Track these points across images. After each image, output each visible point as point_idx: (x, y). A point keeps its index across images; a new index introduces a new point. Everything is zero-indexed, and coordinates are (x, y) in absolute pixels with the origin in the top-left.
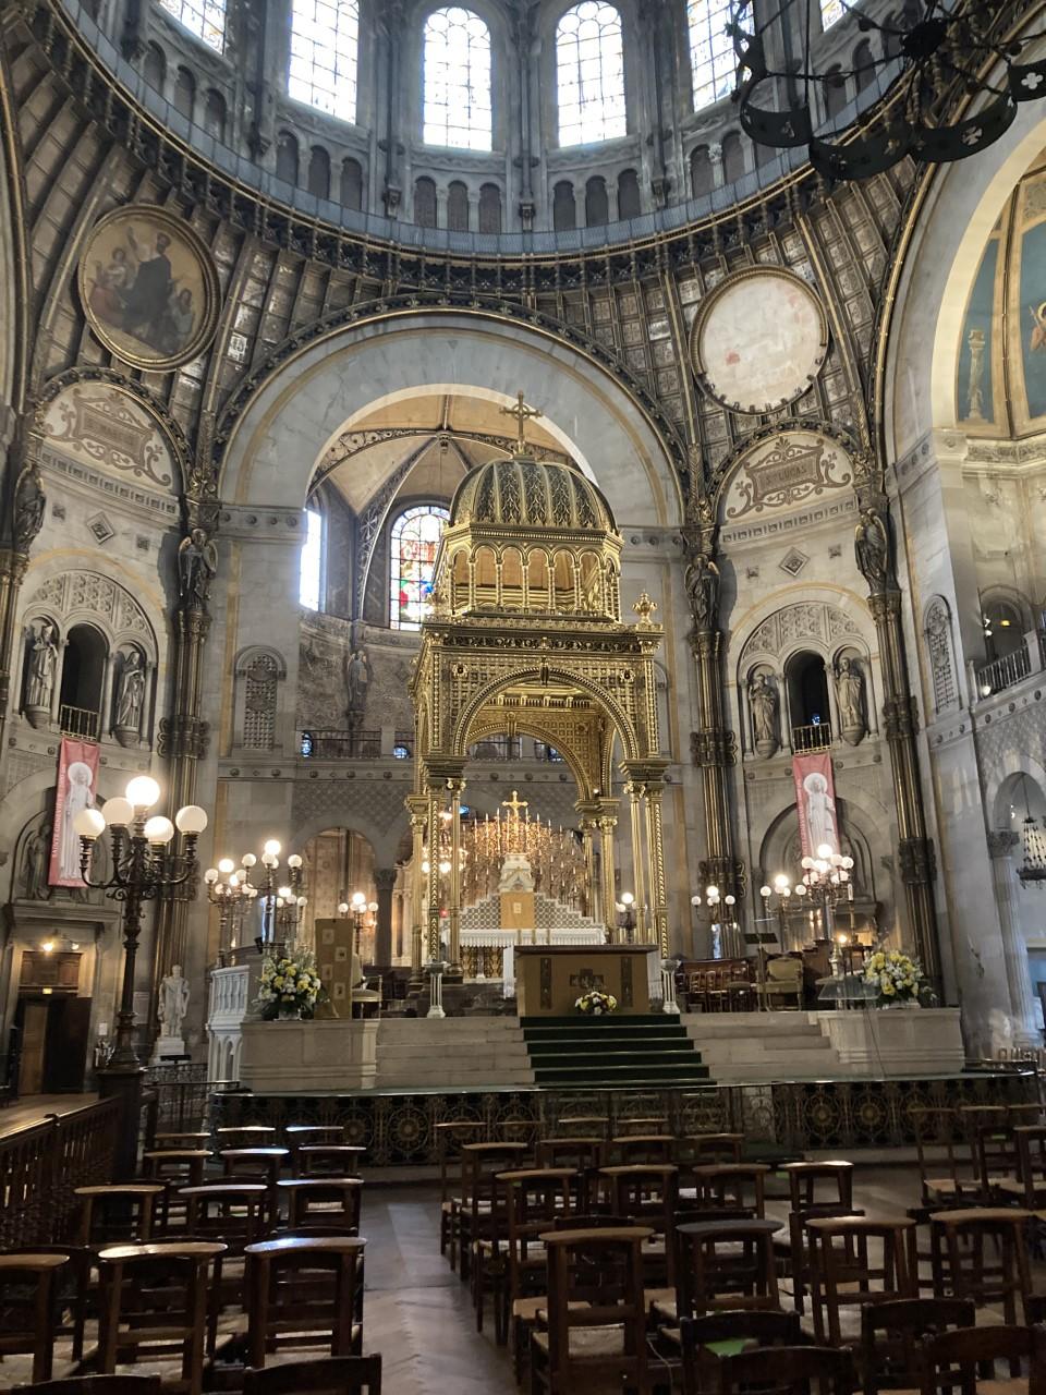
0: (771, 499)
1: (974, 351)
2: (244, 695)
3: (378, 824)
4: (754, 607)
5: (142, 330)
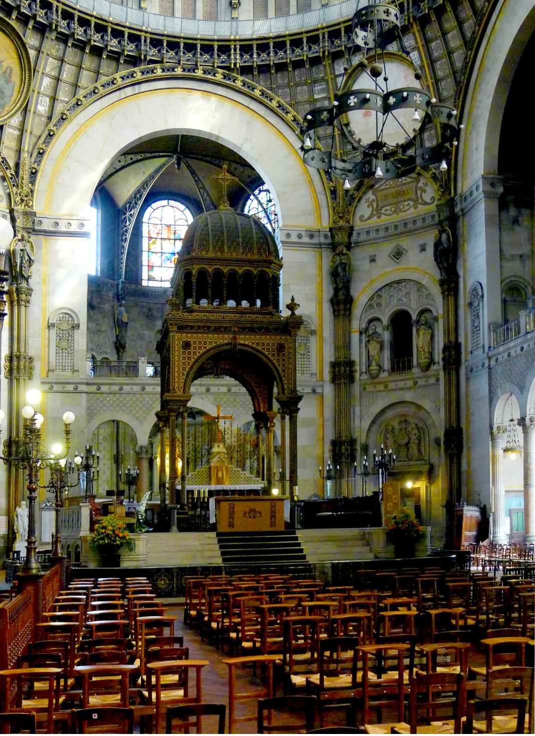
0: (386, 210)
2: (55, 338)
3: (137, 418)
4: (372, 282)
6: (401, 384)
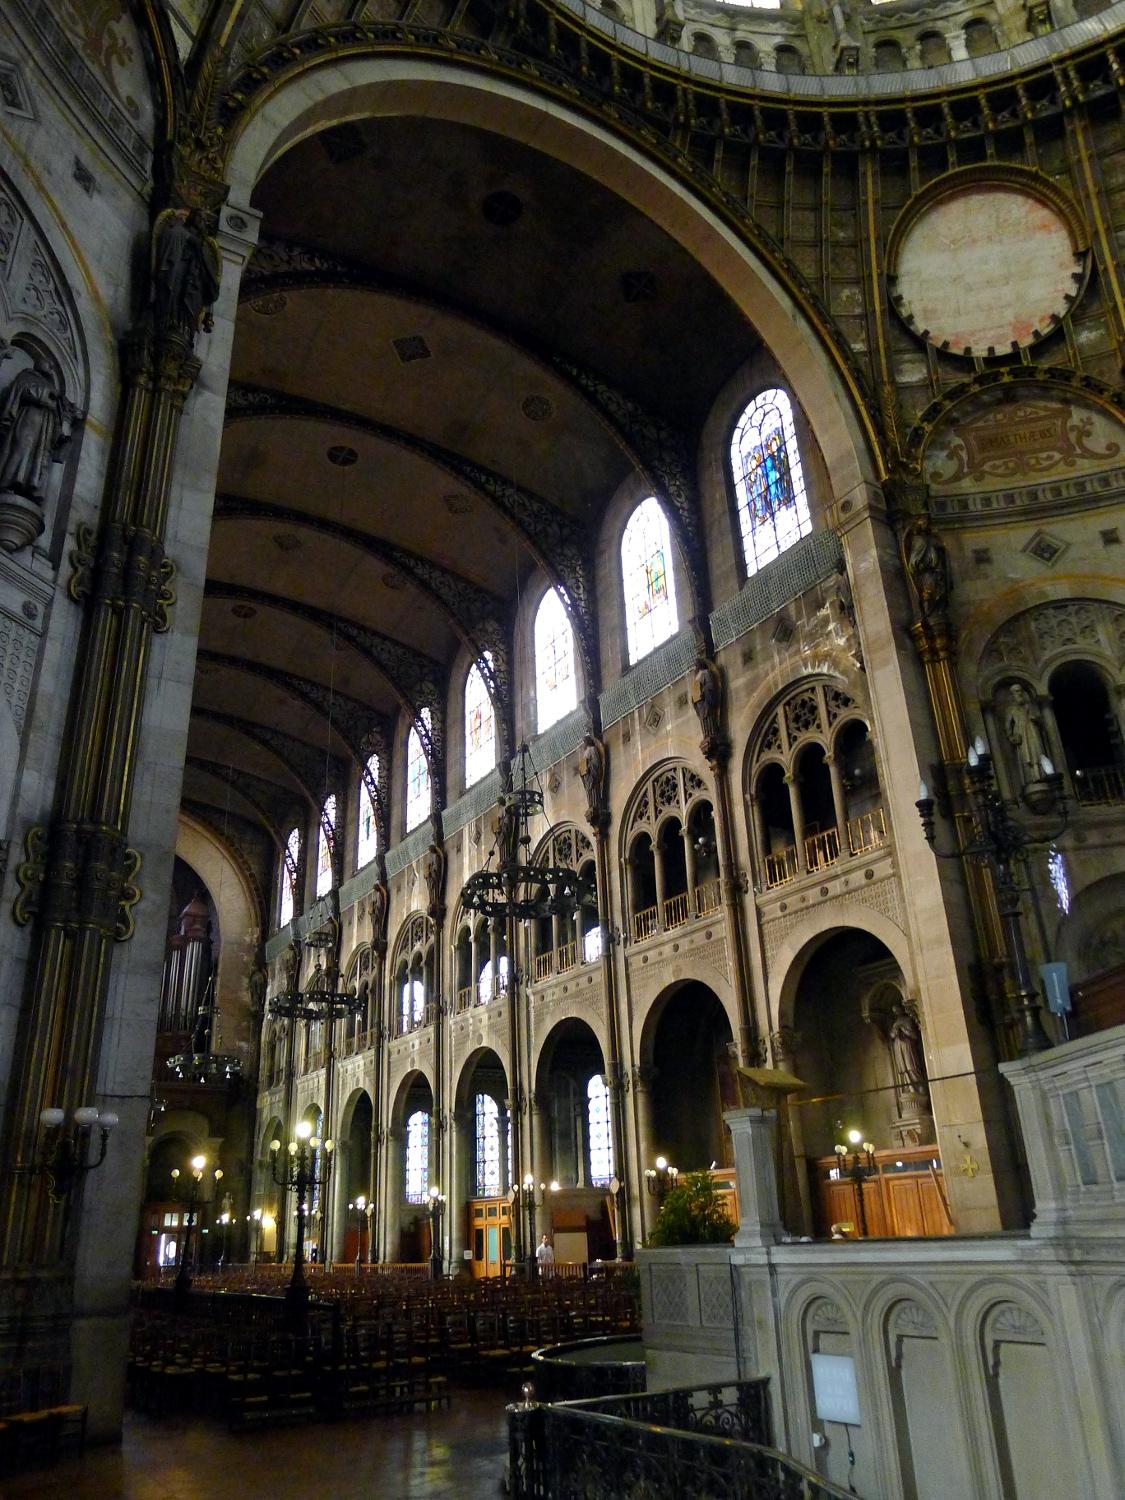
0: (995, 467)
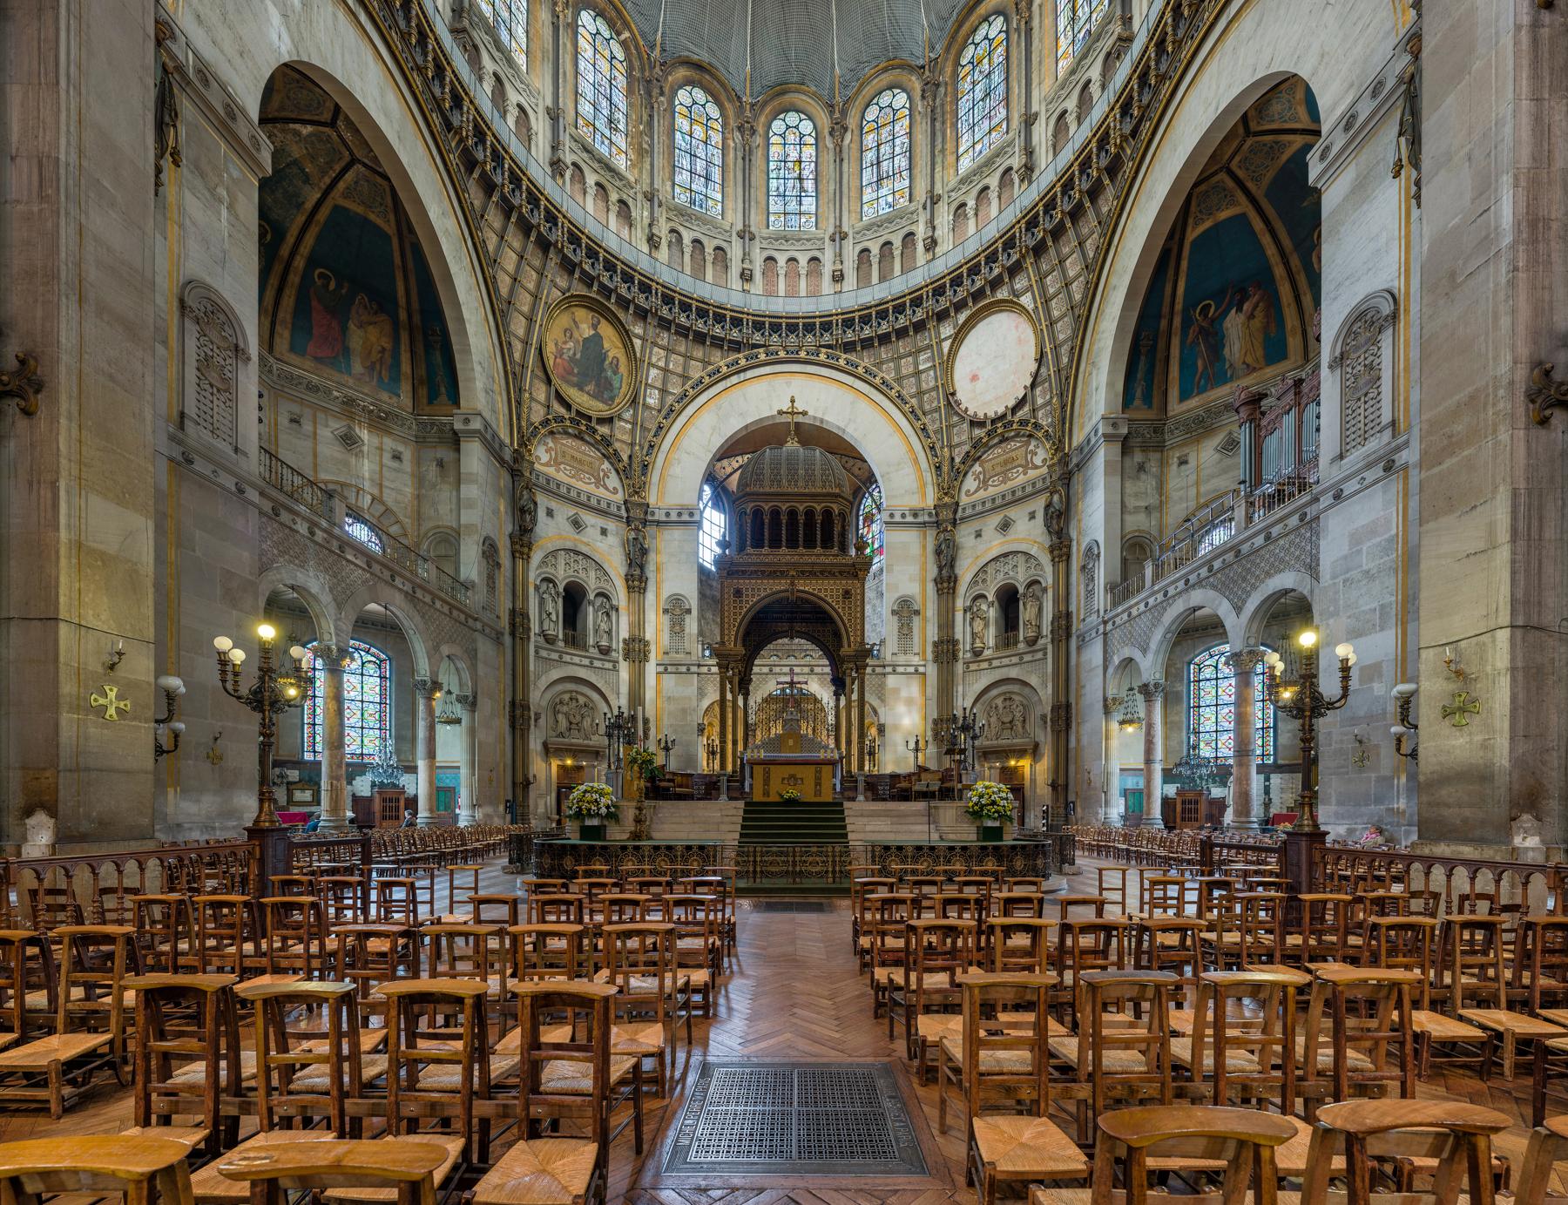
1: (1143, 350)
5: (590, 388)
6: (1006, 661)
